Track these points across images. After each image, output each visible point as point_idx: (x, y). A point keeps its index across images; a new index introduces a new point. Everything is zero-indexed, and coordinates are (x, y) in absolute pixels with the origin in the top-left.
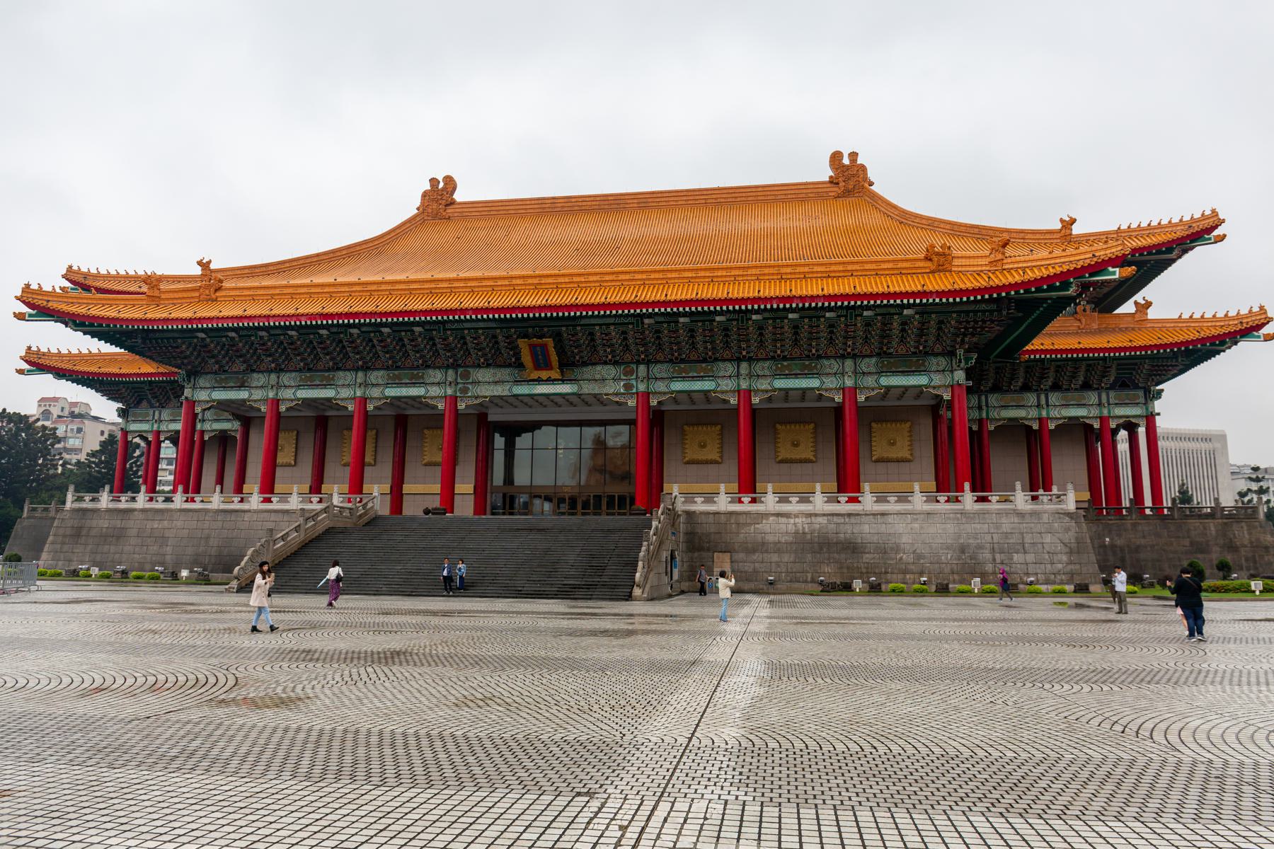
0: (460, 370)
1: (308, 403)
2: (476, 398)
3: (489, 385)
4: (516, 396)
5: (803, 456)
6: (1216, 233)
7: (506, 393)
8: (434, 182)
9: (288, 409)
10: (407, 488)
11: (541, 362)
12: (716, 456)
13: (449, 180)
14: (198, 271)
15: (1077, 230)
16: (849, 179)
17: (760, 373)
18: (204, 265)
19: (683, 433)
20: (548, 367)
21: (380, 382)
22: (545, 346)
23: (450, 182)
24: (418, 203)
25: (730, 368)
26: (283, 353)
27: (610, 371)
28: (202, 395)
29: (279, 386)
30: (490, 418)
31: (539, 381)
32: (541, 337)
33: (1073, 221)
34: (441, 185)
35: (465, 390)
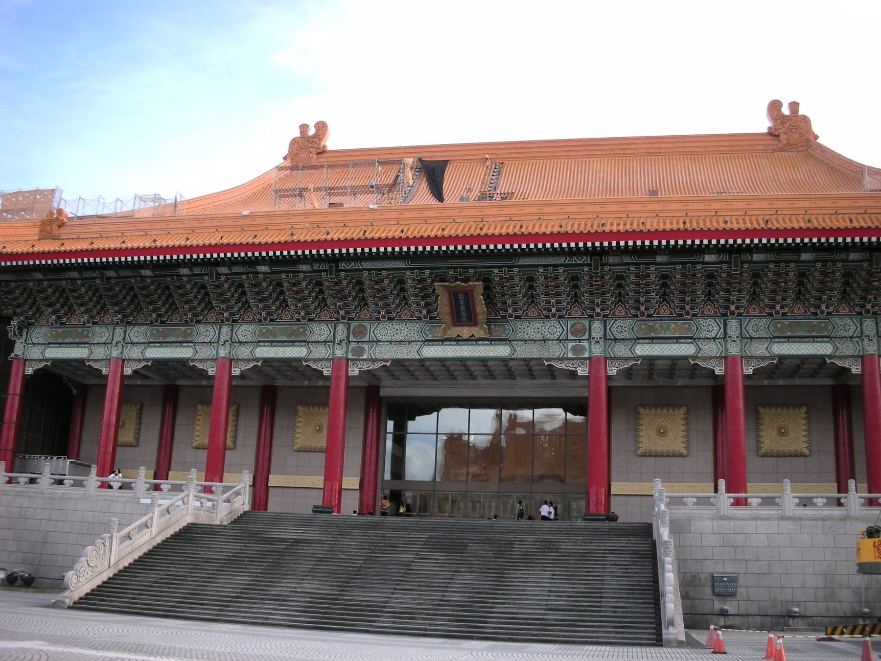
0: (354, 325)
1: (159, 364)
2: (373, 361)
3: (397, 341)
4: (422, 361)
5: (793, 448)
7: (414, 355)
8: (304, 128)
9: (135, 372)
10: (274, 480)
11: (463, 314)
12: (680, 447)
13: (322, 127)
16: (789, 132)
17: (754, 335)
19: (637, 417)
20: (472, 321)
21: (250, 339)
22: (468, 295)
23: (322, 127)
24: (285, 152)
26: (132, 301)
27: (553, 328)
29: (126, 343)
30: (384, 392)
31: (458, 340)
32: (466, 280)
34: (312, 132)
35: (361, 351)
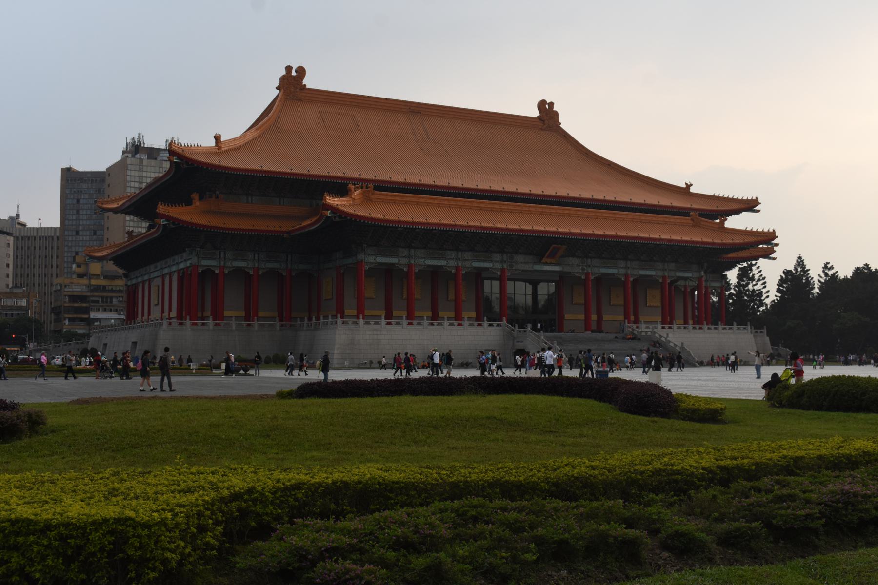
6: (756, 208)
8: (289, 69)
14: (213, 143)
15: (692, 190)
18: (217, 138)
23: (301, 71)
25: (622, 263)
28: (371, 259)
31: (546, 264)
33: (691, 185)
34: (294, 73)
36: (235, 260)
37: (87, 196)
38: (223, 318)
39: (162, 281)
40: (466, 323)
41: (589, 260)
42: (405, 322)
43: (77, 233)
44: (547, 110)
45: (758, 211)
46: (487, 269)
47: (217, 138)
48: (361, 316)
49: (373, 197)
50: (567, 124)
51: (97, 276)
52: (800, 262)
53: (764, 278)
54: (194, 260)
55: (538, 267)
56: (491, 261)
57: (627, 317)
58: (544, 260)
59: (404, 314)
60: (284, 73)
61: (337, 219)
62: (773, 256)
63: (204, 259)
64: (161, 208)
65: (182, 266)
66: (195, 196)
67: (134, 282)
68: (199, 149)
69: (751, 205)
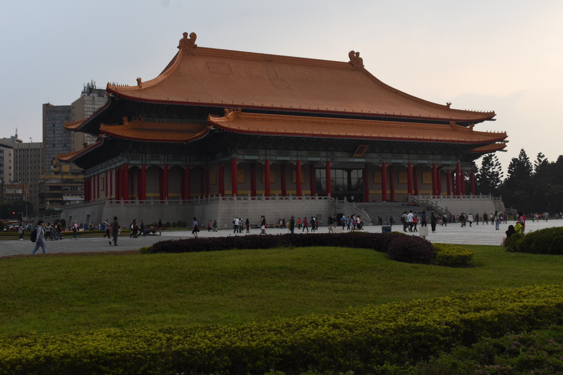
6: (494, 118)
8: (185, 34)
14: (136, 84)
15: (451, 107)
18: (139, 80)
23: (194, 36)
25: (406, 156)
28: (241, 157)
31: (356, 157)
33: (450, 104)
34: (189, 37)
35: (333, 159)
36: (152, 160)
37: (59, 122)
38: (145, 198)
39: (106, 174)
40: (304, 197)
41: (384, 154)
42: (264, 198)
43: (54, 146)
44: (355, 57)
45: (495, 120)
46: (317, 162)
47: (139, 80)
48: (235, 194)
49: (241, 116)
50: (368, 66)
51: (67, 173)
52: (523, 153)
53: (500, 164)
54: (125, 161)
55: (350, 160)
56: (320, 157)
57: (410, 191)
58: (355, 155)
59: (263, 193)
60: (182, 37)
61: (218, 132)
62: (505, 149)
63: (132, 159)
64: (103, 127)
65: (118, 164)
66: (125, 119)
67: (88, 176)
68: (127, 88)
69: (490, 116)
